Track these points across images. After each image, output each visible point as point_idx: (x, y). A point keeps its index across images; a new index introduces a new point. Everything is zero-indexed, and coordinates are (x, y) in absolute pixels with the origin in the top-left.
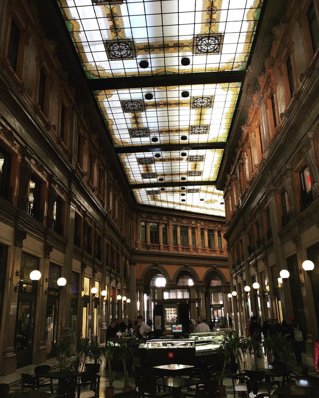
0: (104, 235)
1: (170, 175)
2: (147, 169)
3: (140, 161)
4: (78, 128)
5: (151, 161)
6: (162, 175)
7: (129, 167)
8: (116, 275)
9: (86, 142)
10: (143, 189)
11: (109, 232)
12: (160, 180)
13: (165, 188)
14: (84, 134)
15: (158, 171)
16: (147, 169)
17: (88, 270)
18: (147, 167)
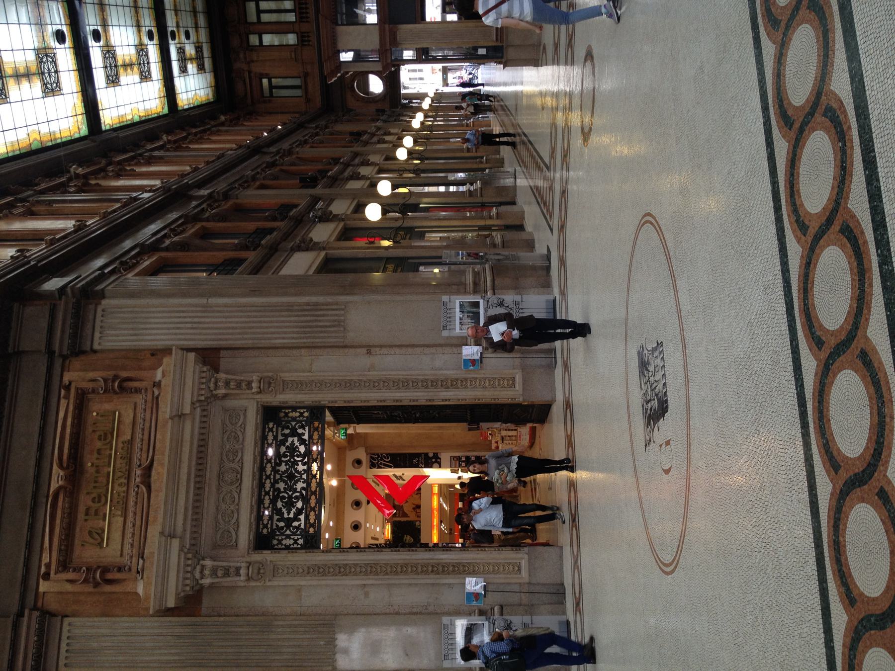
0: (290, 152)
1: (137, 12)
2: (127, 66)
3: (113, 80)
4: (66, 192)
5: (109, 52)
6: (139, 31)
7: (128, 111)
8: (373, 135)
9: (93, 182)
10: (179, 83)
11: (285, 145)
12: (150, 36)
13: (169, 29)
14: (75, 186)
15: (132, 42)
16: (127, 66)
17: (364, 171)
18: (125, 66)
